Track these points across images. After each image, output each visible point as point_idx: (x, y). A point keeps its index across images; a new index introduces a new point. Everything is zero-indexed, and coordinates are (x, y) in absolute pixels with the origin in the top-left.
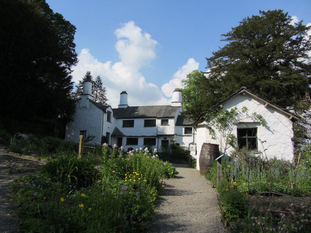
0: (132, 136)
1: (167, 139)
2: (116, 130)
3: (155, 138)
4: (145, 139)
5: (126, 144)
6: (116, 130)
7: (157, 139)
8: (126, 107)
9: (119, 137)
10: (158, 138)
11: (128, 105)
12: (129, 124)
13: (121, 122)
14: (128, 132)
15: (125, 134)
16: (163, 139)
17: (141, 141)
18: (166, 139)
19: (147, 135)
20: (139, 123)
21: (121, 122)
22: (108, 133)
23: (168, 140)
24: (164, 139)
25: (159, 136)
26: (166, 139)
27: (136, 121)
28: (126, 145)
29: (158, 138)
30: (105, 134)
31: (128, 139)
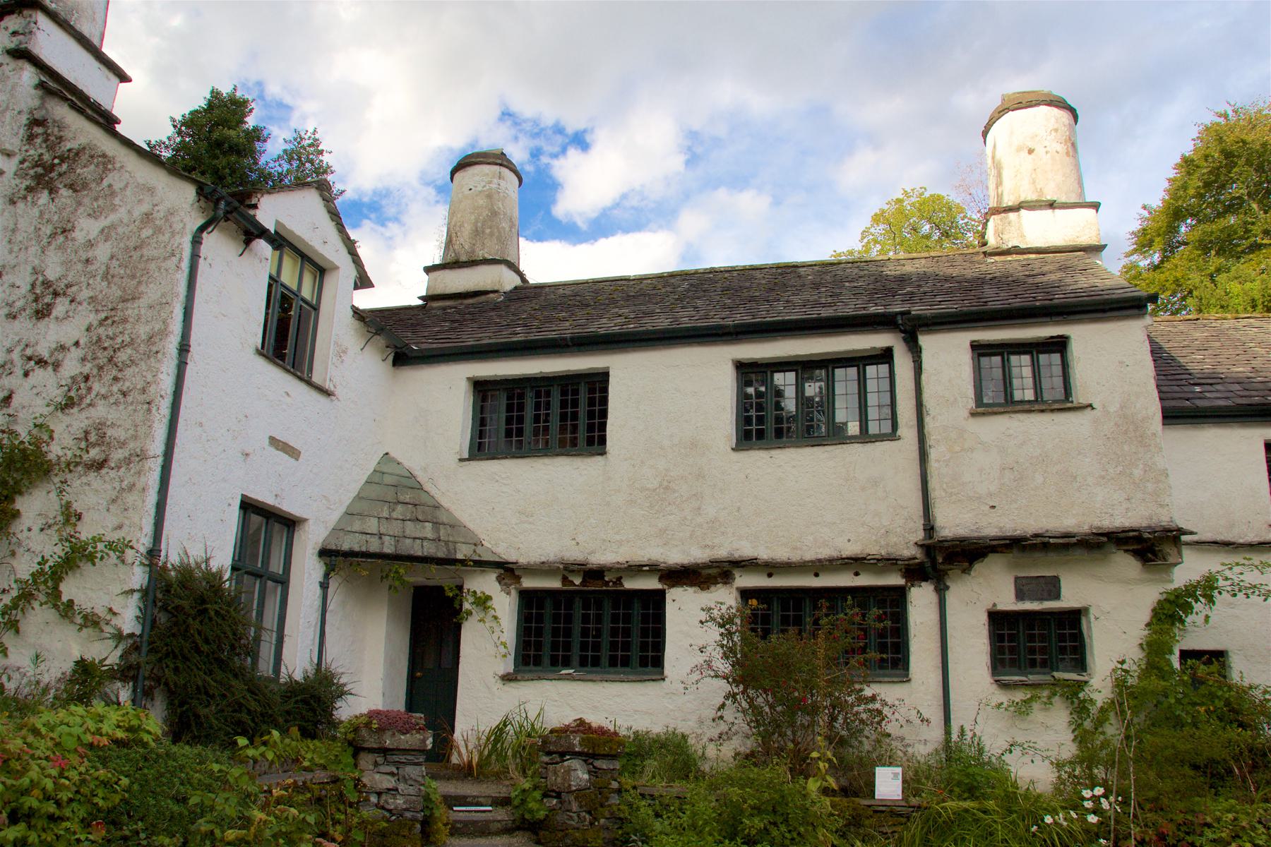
1: (1069, 599)
2: (395, 488)
5: (508, 666)
6: (395, 488)
7: (921, 600)
8: (509, 281)
9: (419, 577)
10: (941, 590)
11: (514, 267)
12: (549, 416)
13: (444, 396)
16: (1008, 602)
17: (692, 624)
18: (1057, 596)
19: (781, 553)
20: (671, 399)
22: (265, 523)
23: (1073, 619)
24: (1020, 596)
25: (944, 559)
26: (1052, 588)
28: (507, 678)
29: (941, 590)
30: (204, 538)
31: (529, 600)
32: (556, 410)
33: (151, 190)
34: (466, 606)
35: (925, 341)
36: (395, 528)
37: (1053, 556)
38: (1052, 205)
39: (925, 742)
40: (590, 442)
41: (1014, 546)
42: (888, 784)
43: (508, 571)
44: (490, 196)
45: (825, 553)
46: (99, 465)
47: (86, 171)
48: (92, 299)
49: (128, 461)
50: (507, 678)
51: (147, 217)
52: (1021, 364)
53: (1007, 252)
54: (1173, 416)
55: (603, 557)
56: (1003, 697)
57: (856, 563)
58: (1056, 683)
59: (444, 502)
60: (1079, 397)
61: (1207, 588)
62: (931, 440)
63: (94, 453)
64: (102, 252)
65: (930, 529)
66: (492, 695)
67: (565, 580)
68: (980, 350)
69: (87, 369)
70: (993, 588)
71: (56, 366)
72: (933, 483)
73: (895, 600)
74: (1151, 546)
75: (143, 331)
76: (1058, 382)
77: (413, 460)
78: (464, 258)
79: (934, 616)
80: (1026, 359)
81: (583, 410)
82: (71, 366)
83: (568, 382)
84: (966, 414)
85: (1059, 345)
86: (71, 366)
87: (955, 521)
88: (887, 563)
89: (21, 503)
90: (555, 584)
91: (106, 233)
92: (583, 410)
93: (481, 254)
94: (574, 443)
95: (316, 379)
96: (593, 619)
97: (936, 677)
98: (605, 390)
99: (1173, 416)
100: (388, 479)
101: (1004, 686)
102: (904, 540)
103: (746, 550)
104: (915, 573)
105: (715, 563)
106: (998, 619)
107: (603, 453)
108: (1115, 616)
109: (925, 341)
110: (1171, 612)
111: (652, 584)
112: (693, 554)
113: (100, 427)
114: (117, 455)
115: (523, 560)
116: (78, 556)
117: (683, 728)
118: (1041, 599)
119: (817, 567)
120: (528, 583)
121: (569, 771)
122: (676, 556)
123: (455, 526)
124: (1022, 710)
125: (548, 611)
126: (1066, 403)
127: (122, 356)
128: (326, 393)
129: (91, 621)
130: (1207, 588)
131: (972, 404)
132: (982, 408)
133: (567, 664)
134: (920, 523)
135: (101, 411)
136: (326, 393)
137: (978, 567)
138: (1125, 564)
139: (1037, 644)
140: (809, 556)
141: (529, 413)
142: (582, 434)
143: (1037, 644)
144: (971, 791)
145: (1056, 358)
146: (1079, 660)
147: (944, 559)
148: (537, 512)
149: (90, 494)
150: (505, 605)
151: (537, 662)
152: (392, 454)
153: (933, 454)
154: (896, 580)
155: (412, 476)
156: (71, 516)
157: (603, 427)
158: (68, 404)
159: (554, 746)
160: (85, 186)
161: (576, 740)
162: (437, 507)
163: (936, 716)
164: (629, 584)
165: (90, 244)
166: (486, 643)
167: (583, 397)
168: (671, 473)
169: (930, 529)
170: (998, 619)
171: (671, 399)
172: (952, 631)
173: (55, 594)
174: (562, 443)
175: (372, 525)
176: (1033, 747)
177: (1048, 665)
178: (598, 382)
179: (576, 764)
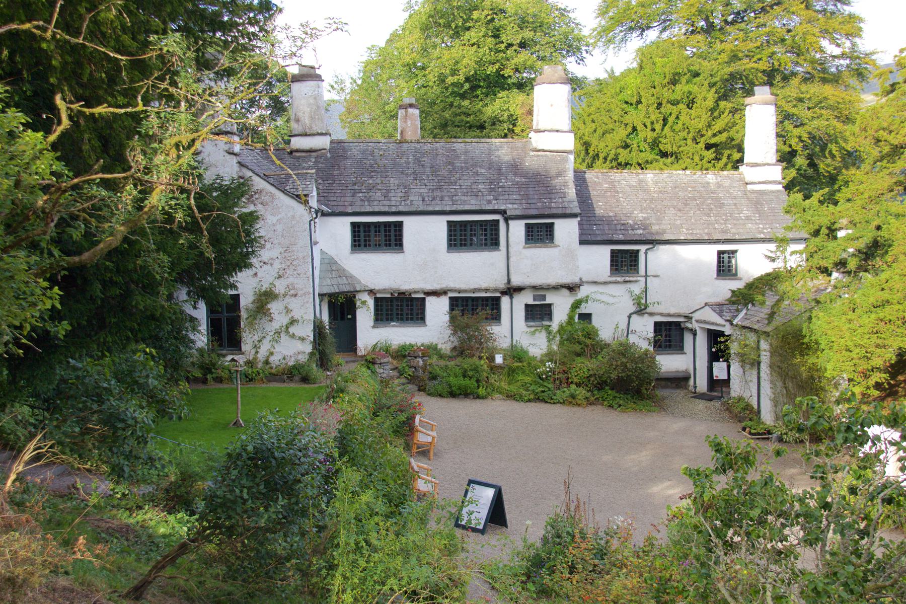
1: (548, 301)
5: (372, 324)
7: (505, 301)
10: (511, 298)
14: (377, 271)
16: (531, 301)
17: (437, 311)
19: (463, 286)
20: (425, 234)
23: (550, 305)
24: (534, 300)
26: (544, 297)
27: (412, 226)
28: (374, 327)
29: (511, 298)
31: (377, 300)
34: (358, 303)
35: (510, 222)
36: (335, 282)
38: (557, 131)
39: (505, 344)
40: (396, 245)
41: (534, 288)
42: (499, 359)
43: (371, 292)
44: (315, 98)
45: (476, 286)
46: (296, 295)
47: (265, 198)
48: (279, 244)
49: (305, 294)
50: (374, 327)
51: (293, 217)
53: (539, 151)
54: (582, 242)
55: (405, 287)
56: (529, 330)
57: (486, 290)
58: (543, 326)
59: (346, 267)
61: (586, 300)
62: (510, 255)
63: (292, 292)
64: (279, 228)
65: (509, 281)
66: (369, 334)
67: (392, 294)
69: (283, 266)
70: (527, 298)
71: (271, 265)
72: (511, 268)
73: (498, 300)
74: (572, 288)
75: (301, 255)
78: (308, 132)
79: (509, 306)
82: (277, 265)
83: (387, 225)
86: (277, 265)
87: (516, 281)
88: (496, 290)
89: (269, 306)
90: (389, 296)
91: (279, 221)
93: (316, 129)
96: (401, 307)
97: (509, 324)
98: (401, 230)
99: (582, 242)
100: (327, 261)
101: (528, 326)
102: (501, 284)
103: (452, 285)
104: (504, 293)
105: (441, 289)
106: (527, 306)
108: (561, 306)
109: (510, 222)
110: (576, 305)
111: (422, 296)
112: (436, 286)
113: (292, 284)
114: (300, 293)
115: (377, 288)
116: (293, 322)
117: (434, 341)
119: (475, 291)
120: (378, 296)
122: (429, 287)
123: (352, 277)
124: (533, 333)
125: (384, 304)
127: (295, 263)
129: (303, 339)
130: (586, 300)
133: (392, 320)
134: (506, 278)
135: (291, 280)
137: (523, 292)
138: (565, 292)
139: (538, 313)
140: (472, 287)
142: (393, 242)
143: (538, 313)
144: (520, 360)
146: (550, 319)
147: (512, 291)
149: (294, 304)
150: (371, 303)
153: (511, 260)
154: (498, 295)
156: (288, 310)
157: (401, 240)
158: (280, 277)
160: (267, 204)
161: (420, 354)
162: (344, 270)
163: (509, 335)
164: (413, 296)
165: (274, 225)
166: (365, 317)
167: (393, 229)
169: (509, 281)
170: (527, 306)
171: (425, 234)
172: (513, 311)
173: (287, 332)
174: (386, 245)
175: (329, 282)
176: (537, 344)
177: (542, 319)
178: (400, 225)
179: (420, 359)
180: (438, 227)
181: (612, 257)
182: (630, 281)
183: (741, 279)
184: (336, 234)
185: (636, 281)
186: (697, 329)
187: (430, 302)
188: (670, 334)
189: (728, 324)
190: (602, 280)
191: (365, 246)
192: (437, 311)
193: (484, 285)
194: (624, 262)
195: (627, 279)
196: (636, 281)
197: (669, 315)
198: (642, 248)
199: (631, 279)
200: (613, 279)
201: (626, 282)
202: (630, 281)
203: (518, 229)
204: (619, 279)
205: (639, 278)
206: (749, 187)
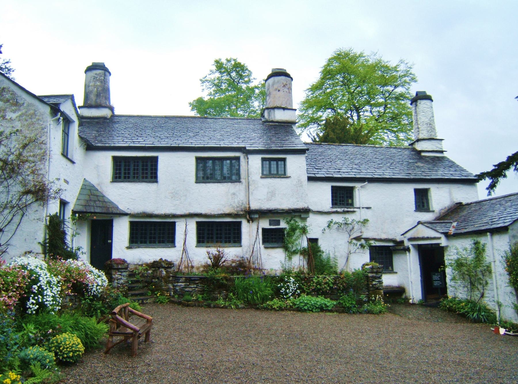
0: (151, 216)
3: (238, 220)
4: (199, 225)
5: (127, 243)
15: (123, 207)
17: (186, 232)
18: (279, 225)
20: (176, 168)
21: (105, 161)
24: (270, 225)
25: (252, 215)
27: (165, 160)
28: (128, 248)
31: (133, 225)
32: (140, 167)
33: (33, 105)
37: (279, 215)
40: (152, 178)
50: (128, 248)
52: (274, 164)
60: (288, 173)
68: (263, 160)
76: (283, 169)
77: (94, 181)
80: (275, 162)
81: (149, 167)
84: (259, 177)
85: (284, 160)
87: (254, 206)
92: (149, 167)
94: (147, 178)
95: (69, 157)
96: (153, 230)
99: (310, 179)
100: (88, 188)
106: (264, 230)
107: (157, 182)
109: (250, 157)
118: (275, 225)
121: (162, 271)
126: (284, 176)
128: (73, 162)
131: (261, 175)
132: (264, 176)
136: (73, 162)
141: (132, 168)
142: (149, 175)
145: (283, 162)
148: (132, 198)
151: (136, 242)
152: (87, 179)
155: (94, 186)
157: (156, 173)
159: (156, 265)
162: (104, 196)
167: (149, 164)
168: (177, 189)
170: (264, 230)
179: (163, 270)
180: (189, 160)
181: (332, 190)
182: (348, 212)
183: (433, 211)
184: (100, 167)
185: (354, 212)
186: (411, 247)
187: (180, 227)
188: (384, 254)
189: (443, 237)
190: (326, 210)
191: (125, 178)
192: (186, 232)
193: (227, 211)
194: (343, 197)
195: (346, 209)
196: (354, 212)
197: (381, 240)
198: (357, 185)
199: (349, 210)
200: (335, 210)
201: (344, 212)
202: (348, 212)
203: (255, 161)
204: (339, 210)
205: (355, 210)
206: (423, 154)
